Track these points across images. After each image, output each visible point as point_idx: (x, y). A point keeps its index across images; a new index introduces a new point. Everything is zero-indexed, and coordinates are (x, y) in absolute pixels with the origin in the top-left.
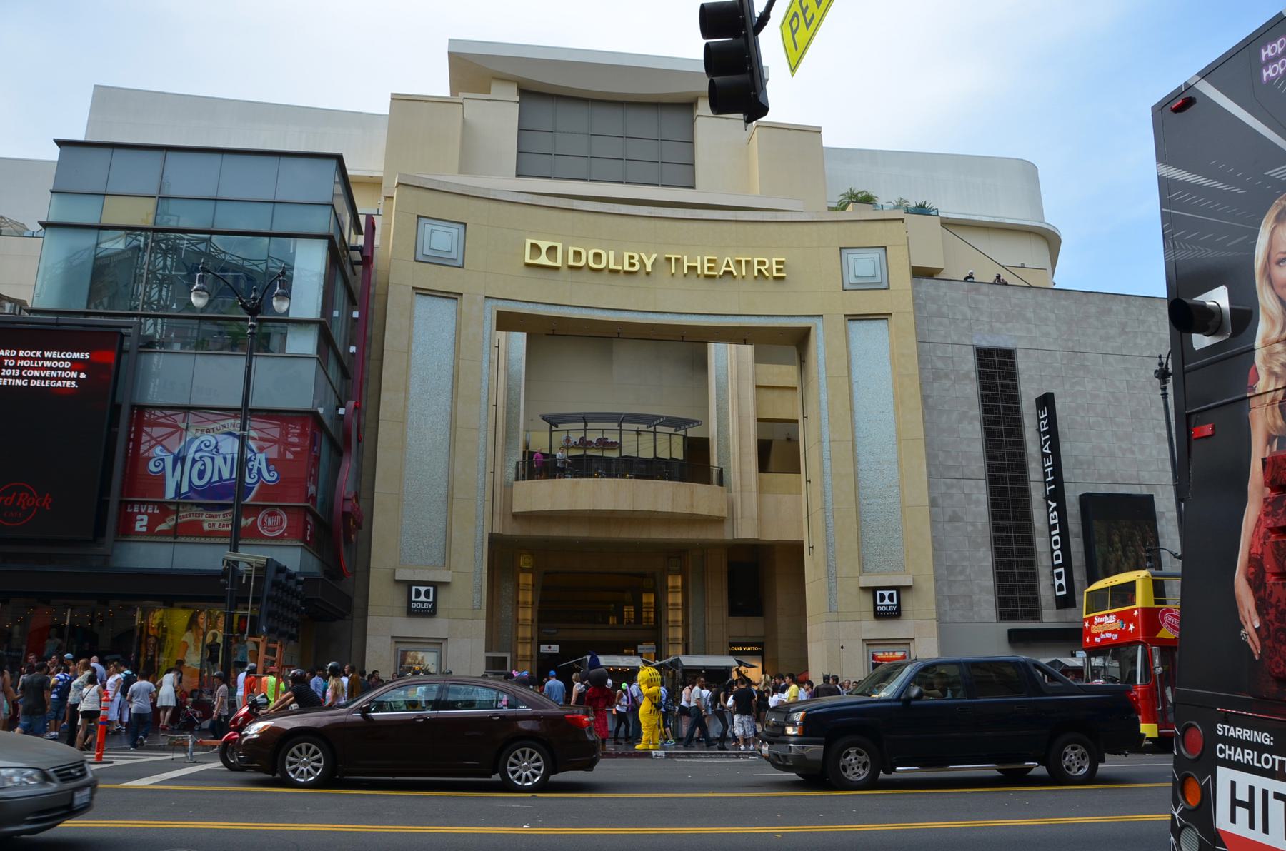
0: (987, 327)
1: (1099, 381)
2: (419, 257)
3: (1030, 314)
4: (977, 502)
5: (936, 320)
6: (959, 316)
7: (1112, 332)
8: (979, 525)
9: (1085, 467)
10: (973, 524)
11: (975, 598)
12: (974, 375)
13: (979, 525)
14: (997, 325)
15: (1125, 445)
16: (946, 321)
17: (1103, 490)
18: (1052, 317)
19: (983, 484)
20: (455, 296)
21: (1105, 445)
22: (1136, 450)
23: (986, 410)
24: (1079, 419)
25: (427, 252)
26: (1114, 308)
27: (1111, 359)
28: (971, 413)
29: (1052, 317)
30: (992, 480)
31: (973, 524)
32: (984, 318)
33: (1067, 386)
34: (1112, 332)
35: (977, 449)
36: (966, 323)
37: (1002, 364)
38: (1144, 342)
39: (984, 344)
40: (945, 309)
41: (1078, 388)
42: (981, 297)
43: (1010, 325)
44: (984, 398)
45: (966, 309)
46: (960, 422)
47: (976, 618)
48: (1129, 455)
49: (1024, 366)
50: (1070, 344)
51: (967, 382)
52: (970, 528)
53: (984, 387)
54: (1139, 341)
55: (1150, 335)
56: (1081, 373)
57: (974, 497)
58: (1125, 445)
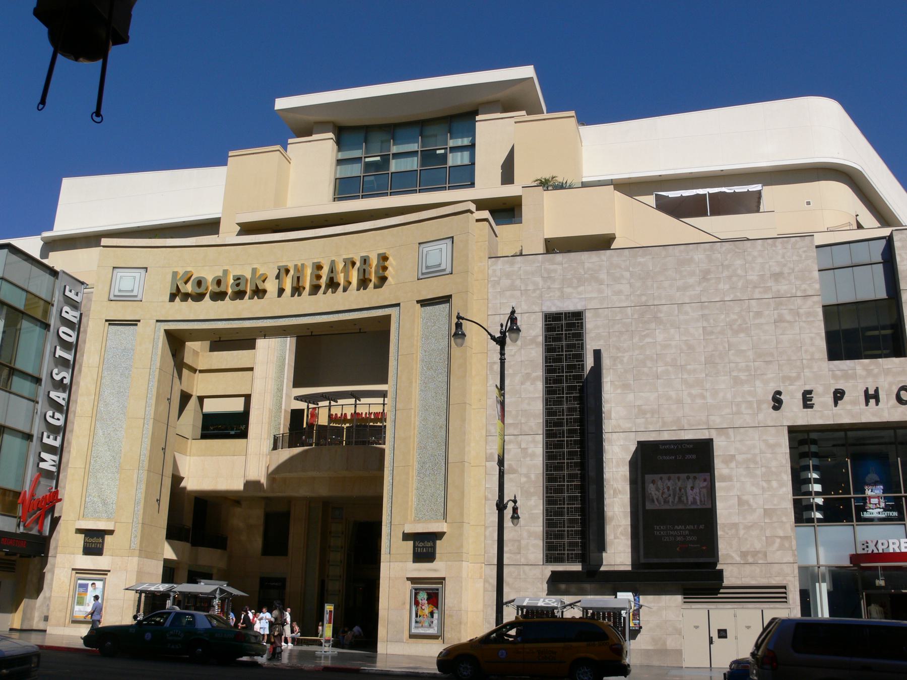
0: (558, 294)
1: (672, 331)
2: (112, 298)
3: (603, 276)
4: (533, 455)
5: (508, 293)
6: (531, 287)
7: (691, 281)
8: (533, 477)
9: (648, 415)
10: (527, 476)
11: (523, 542)
12: (540, 339)
13: (533, 477)
14: (568, 290)
15: (694, 391)
16: (518, 293)
17: (666, 437)
18: (627, 274)
19: (540, 439)
20: (134, 323)
21: (673, 394)
22: (708, 394)
23: (549, 370)
24: (646, 370)
25: (117, 293)
26: (696, 257)
27: (687, 308)
28: (534, 374)
29: (627, 274)
30: (549, 434)
31: (527, 476)
32: (556, 285)
33: (636, 340)
34: (691, 281)
35: (538, 407)
36: (538, 292)
37: (570, 326)
38: (727, 287)
39: (554, 309)
40: (518, 282)
41: (648, 340)
42: (552, 267)
43: (581, 289)
44: (547, 360)
45: (538, 280)
46: (522, 383)
47: (523, 561)
48: (699, 401)
49: (591, 325)
50: (644, 299)
51: (533, 346)
52: (523, 480)
53: (549, 349)
54: (721, 286)
55: (734, 279)
56: (653, 326)
57: (530, 451)
58: (694, 391)
